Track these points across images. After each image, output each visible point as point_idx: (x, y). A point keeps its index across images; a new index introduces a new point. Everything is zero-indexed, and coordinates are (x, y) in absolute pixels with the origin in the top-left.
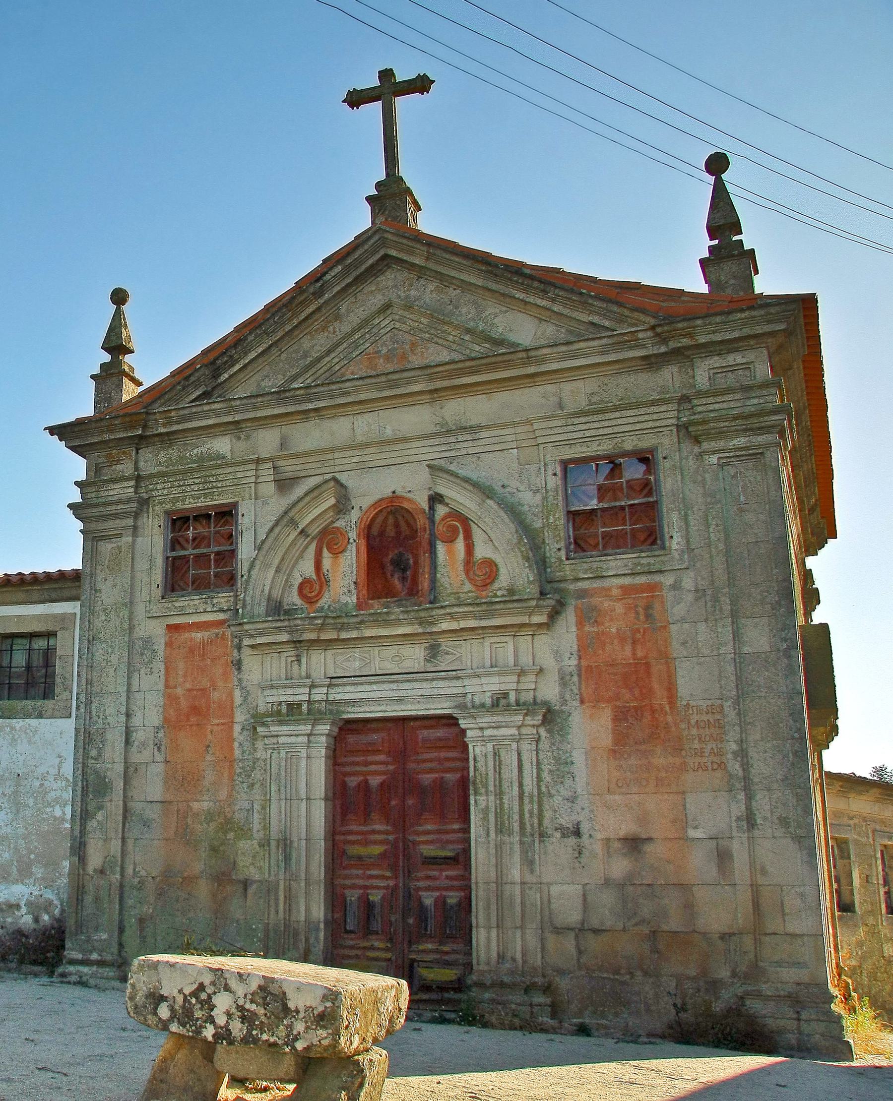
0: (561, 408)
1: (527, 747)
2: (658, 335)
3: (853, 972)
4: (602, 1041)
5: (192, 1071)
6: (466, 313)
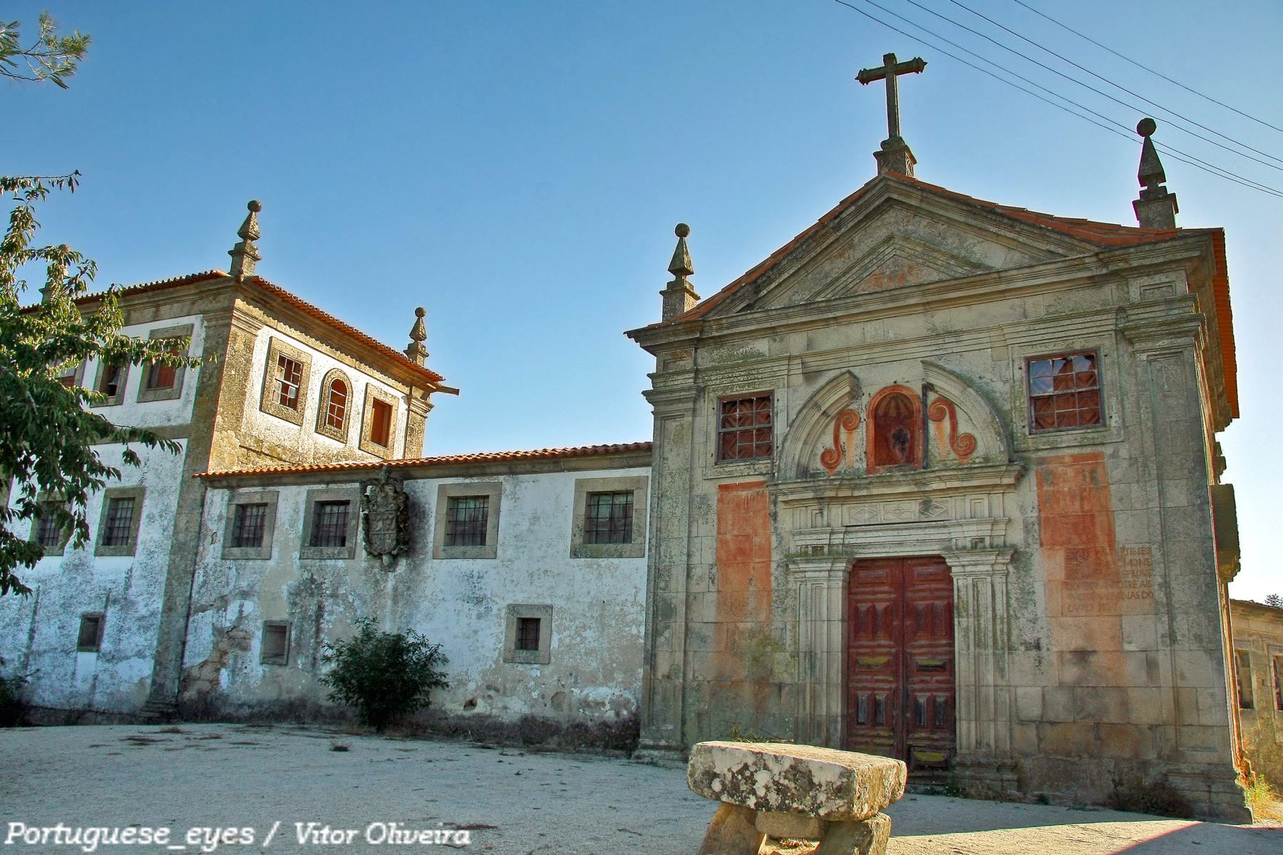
0: (1025, 317)
1: (999, 580)
2: (1100, 260)
3: (1252, 755)
4: (1057, 808)
5: (739, 832)
6: (952, 243)
